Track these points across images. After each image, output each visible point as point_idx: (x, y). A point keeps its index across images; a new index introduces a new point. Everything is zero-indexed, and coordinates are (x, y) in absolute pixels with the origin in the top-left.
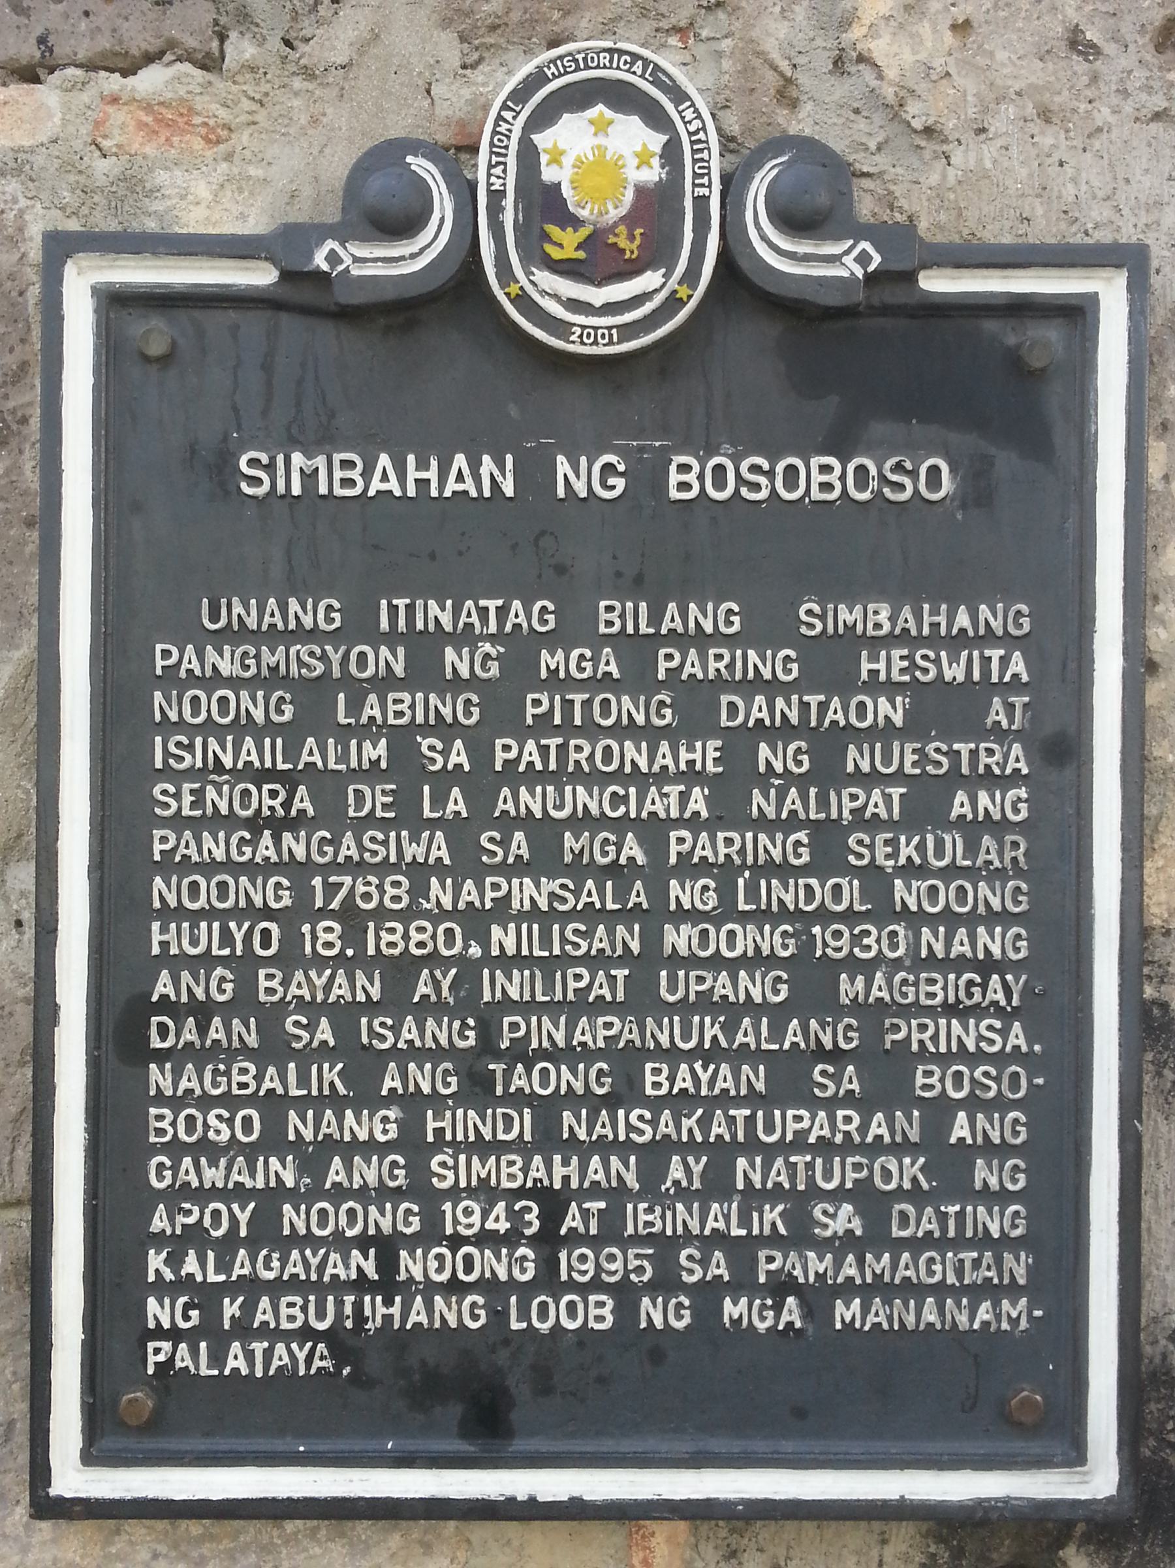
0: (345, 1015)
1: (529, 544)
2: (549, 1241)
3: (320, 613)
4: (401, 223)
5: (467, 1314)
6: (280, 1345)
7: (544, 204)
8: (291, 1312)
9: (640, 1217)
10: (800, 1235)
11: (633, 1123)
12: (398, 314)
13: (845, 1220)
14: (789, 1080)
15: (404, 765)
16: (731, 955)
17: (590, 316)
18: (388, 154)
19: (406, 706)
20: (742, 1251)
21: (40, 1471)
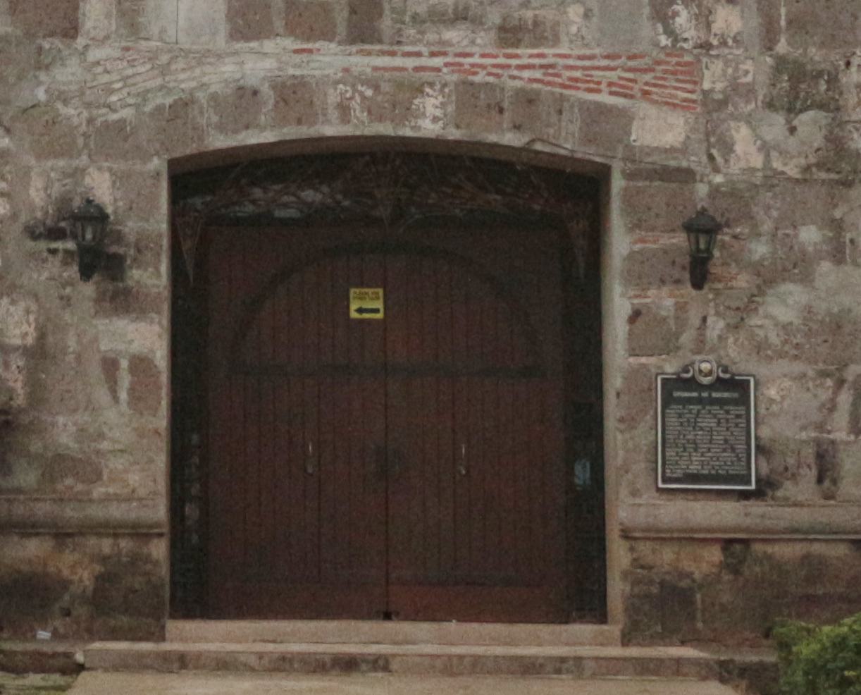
0: (684, 444)
1: (699, 401)
2: (702, 466)
3: (681, 407)
4: (687, 372)
5: (695, 472)
6: (679, 473)
7: (701, 371)
8: (679, 471)
9: (712, 463)
10: (726, 464)
11: (710, 454)
12: (687, 380)
13: (729, 463)
14: (724, 450)
15: (688, 421)
16: (718, 438)
17: (706, 380)
18: (687, 366)
19: (688, 416)
20: (720, 466)
21: (657, 483)
